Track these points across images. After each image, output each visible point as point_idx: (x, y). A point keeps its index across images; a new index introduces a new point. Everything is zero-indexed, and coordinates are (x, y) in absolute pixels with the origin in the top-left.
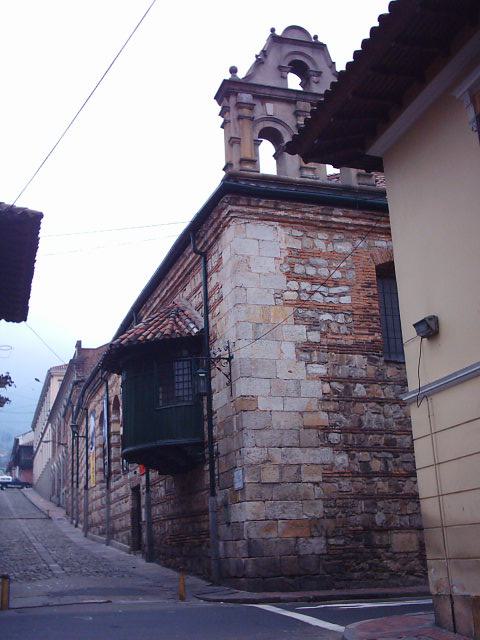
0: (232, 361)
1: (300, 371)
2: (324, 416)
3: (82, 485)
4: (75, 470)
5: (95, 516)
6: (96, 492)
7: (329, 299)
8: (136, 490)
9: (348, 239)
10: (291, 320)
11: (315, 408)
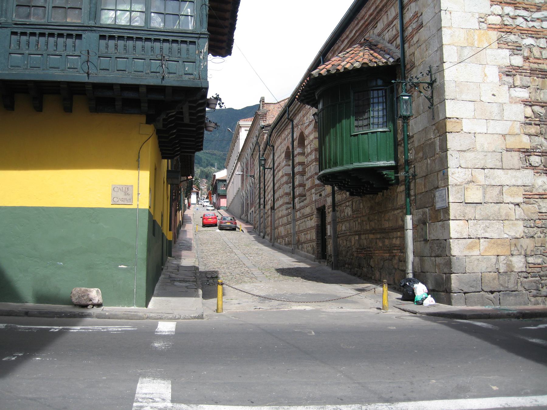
0: (435, 85)
1: (504, 94)
2: (526, 139)
3: (268, 207)
4: (262, 196)
5: (282, 230)
6: (282, 211)
7: (531, 24)
8: (321, 211)
10: (495, 45)
11: (517, 131)
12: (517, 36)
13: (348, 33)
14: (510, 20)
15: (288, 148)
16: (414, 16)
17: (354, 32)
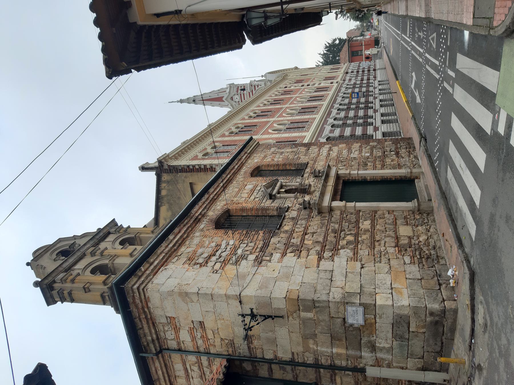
9: (192, 238)
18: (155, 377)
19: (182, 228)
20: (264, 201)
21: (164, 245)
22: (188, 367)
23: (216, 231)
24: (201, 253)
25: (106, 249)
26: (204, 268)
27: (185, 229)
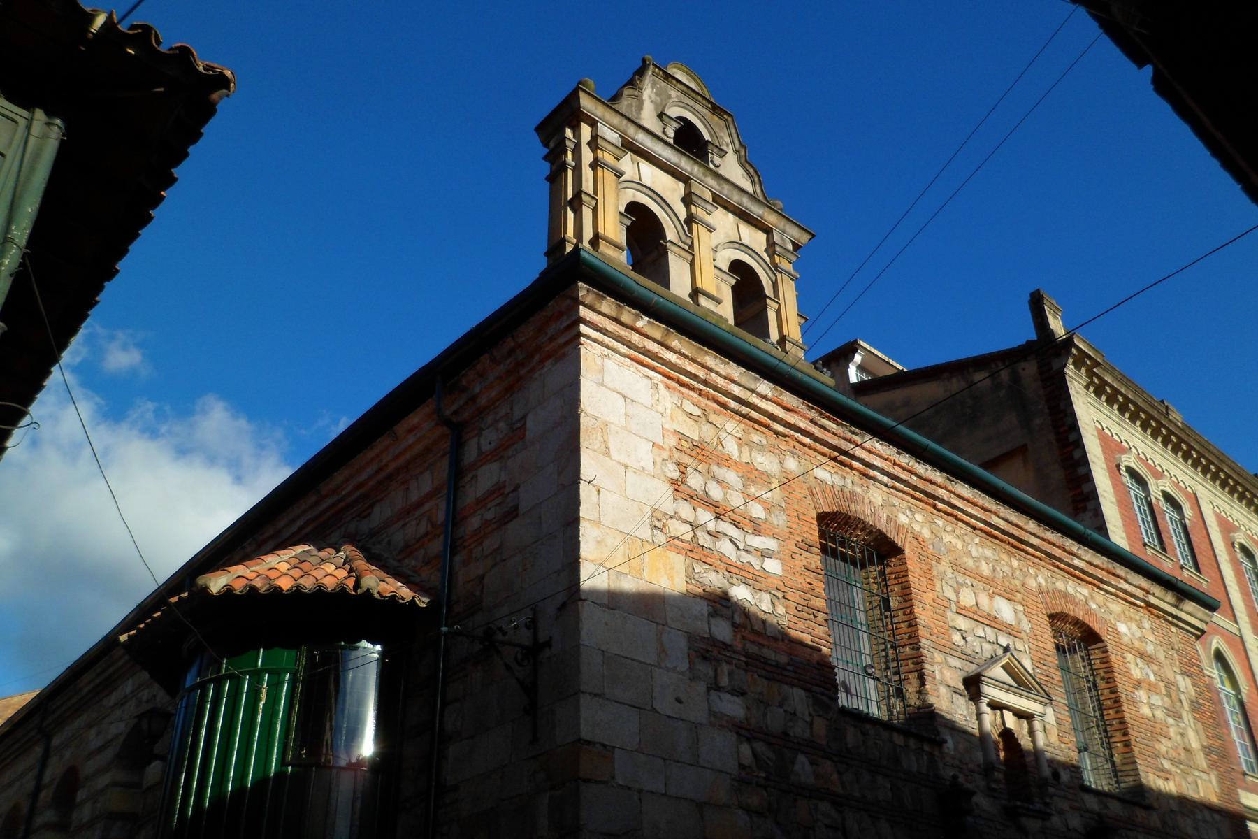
7: (746, 558)
9: (772, 450)
12: (720, 576)
13: (282, 523)
14: (708, 538)
15: (16, 808)
16: (490, 494)
17: (299, 523)
18: (401, 428)
19: (804, 416)
20: (955, 662)
21: (735, 371)
22: (427, 507)
23: (815, 516)
24: (721, 478)
25: (711, 229)
26: (666, 490)
27: (803, 424)
